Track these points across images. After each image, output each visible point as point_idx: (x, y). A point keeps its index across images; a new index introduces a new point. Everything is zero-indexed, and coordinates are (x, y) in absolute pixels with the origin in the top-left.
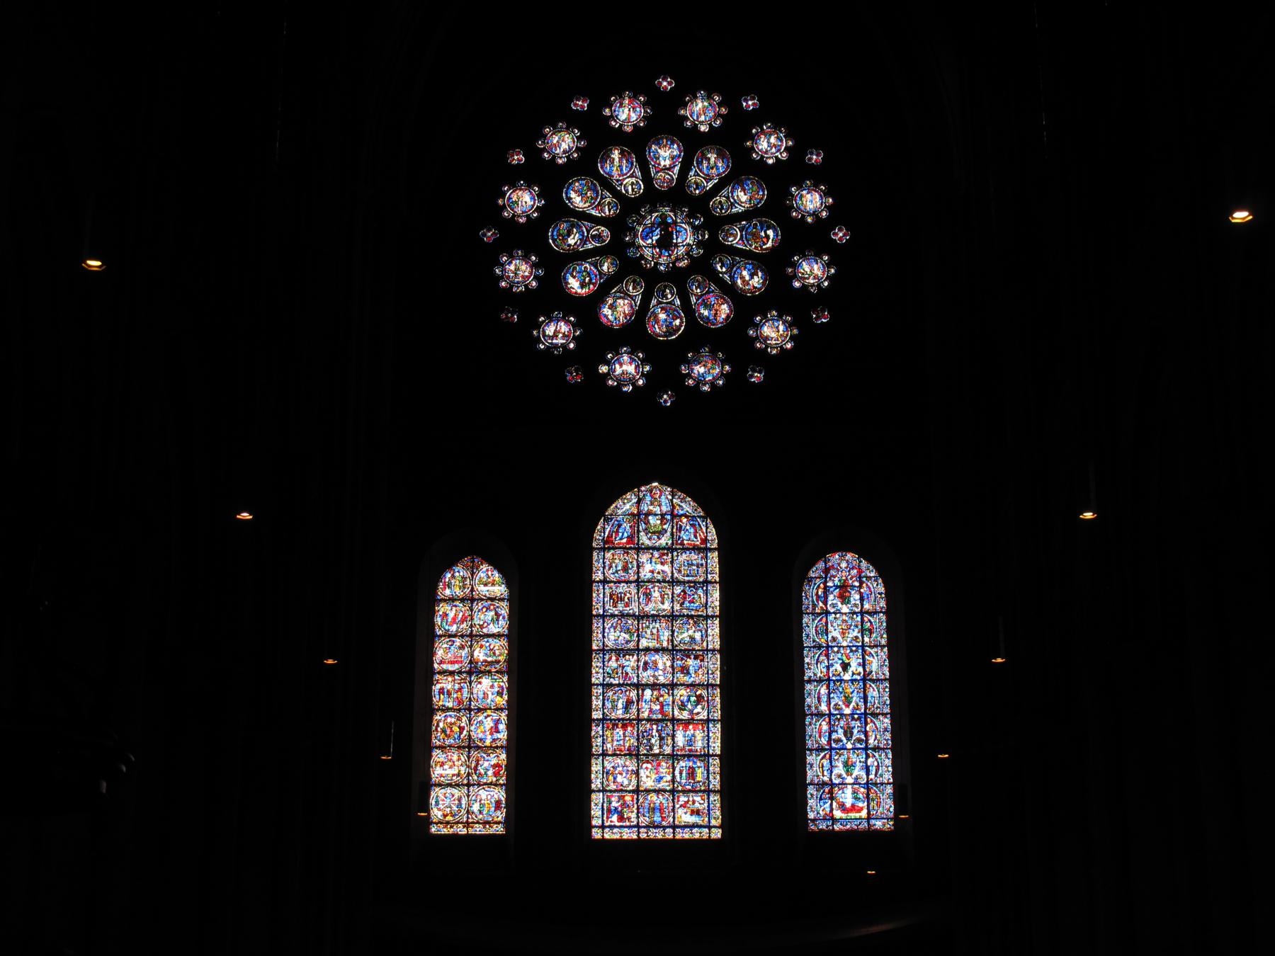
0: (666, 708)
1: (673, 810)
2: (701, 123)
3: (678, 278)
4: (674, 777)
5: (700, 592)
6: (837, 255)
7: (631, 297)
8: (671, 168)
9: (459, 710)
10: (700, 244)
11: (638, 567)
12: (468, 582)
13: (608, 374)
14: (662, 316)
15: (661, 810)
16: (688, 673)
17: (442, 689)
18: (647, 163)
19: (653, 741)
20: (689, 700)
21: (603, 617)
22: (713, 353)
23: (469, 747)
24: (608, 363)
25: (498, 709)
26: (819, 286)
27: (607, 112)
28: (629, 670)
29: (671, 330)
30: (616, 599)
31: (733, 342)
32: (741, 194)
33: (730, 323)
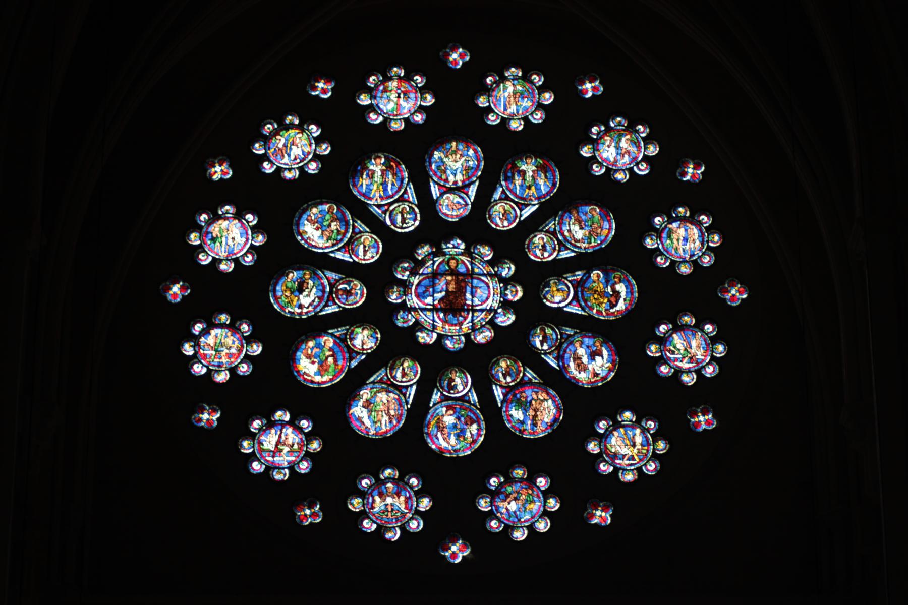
2: (512, 117)
3: (476, 360)
14: (449, 420)
31: (564, 459)
32: (575, 228)
33: (559, 430)
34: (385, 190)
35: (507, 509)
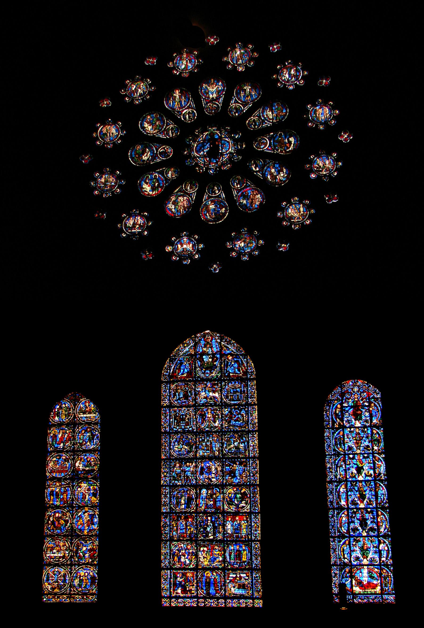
0: (218, 504)
1: (224, 585)
2: (239, 65)
4: (225, 558)
5: (243, 412)
6: (343, 152)
7: (189, 194)
8: (217, 99)
9: (65, 507)
10: (238, 152)
11: (196, 395)
12: (71, 411)
13: (172, 252)
14: (212, 207)
15: (215, 583)
16: (235, 476)
17: (52, 491)
18: (200, 97)
19: (208, 529)
20: (235, 497)
21: (169, 433)
22: (250, 233)
23: (72, 536)
24: (172, 244)
25: (93, 507)
26: (330, 175)
27: (171, 65)
28: (189, 474)
29: (219, 216)
30: (179, 419)
31: (265, 221)
34: (181, 104)
35: (239, 245)
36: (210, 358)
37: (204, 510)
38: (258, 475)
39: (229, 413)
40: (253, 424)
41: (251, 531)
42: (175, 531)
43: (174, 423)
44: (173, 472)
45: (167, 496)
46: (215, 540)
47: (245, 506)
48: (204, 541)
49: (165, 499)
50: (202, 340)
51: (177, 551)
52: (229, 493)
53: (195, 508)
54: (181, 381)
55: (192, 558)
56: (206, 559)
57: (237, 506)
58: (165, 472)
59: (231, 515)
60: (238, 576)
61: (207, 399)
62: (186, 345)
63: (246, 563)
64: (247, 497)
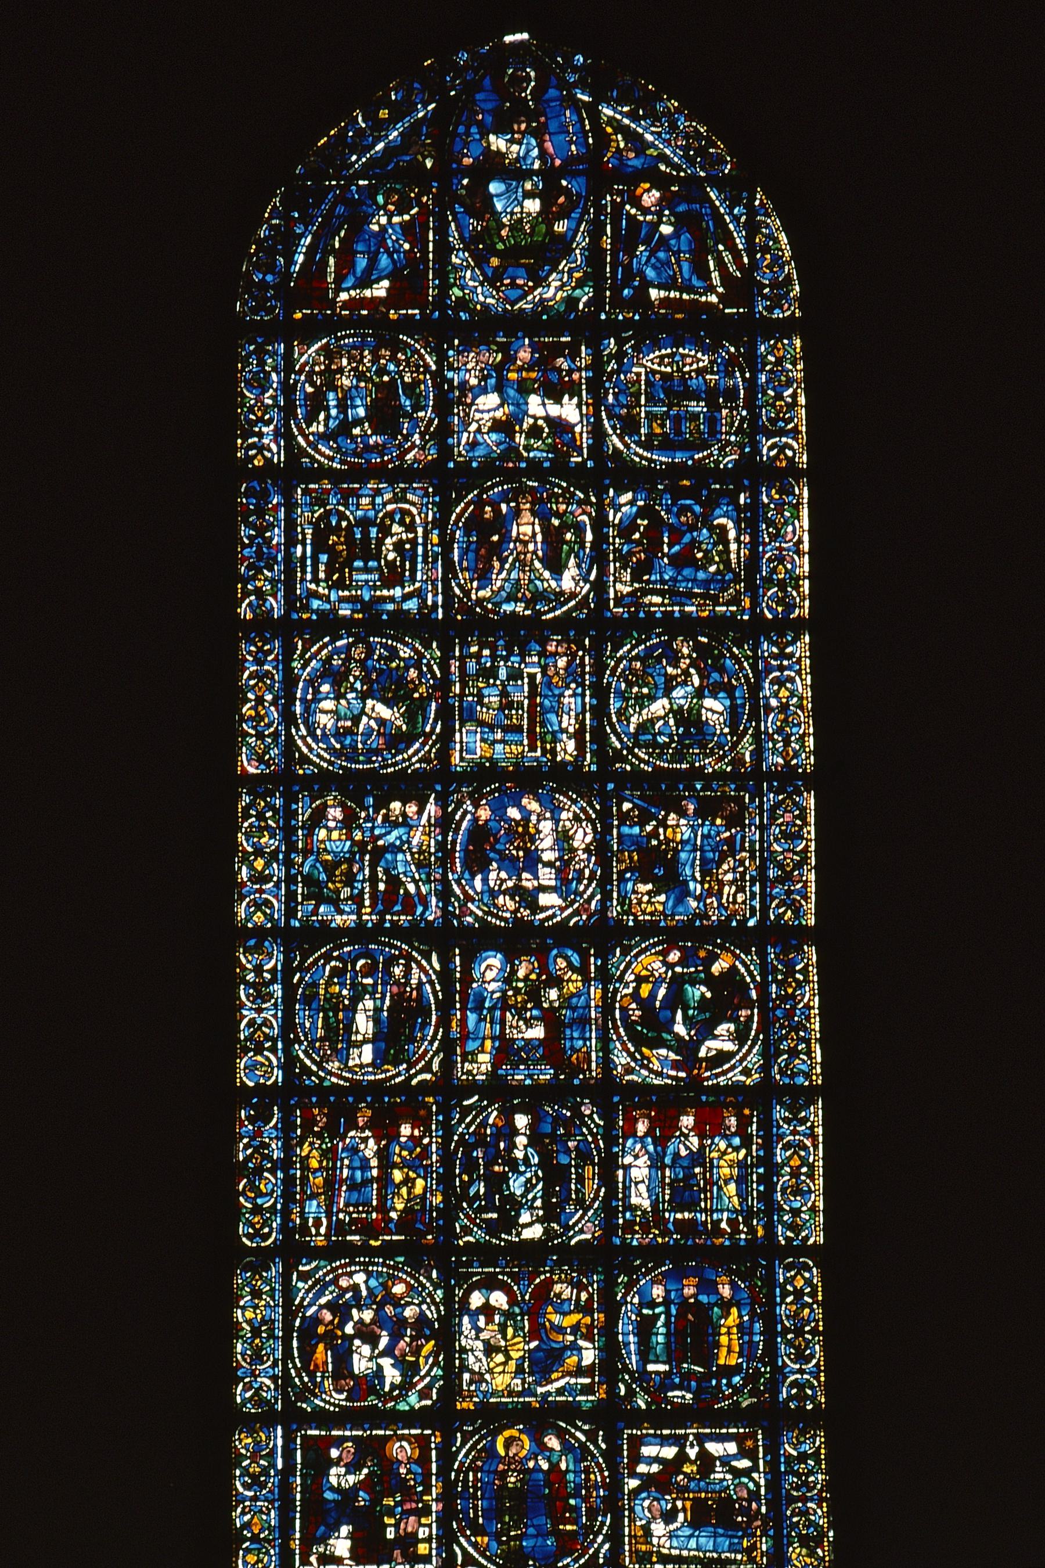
11: (444, 407)
19: (516, 1186)
20: (676, 999)
36: (528, 195)
37: (492, 1075)
38: (812, 877)
39: (641, 513)
40: (782, 585)
41: (767, 1197)
42: (314, 1196)
43: (315, 571)
44: (306, 852)
45: (271, 995)
46: (555, 1250)
47: (730, 1055)
48: (483, 1253)
49: (259, 1011)
50: (481, 89)
51: (328, 1316)
52: (640, 980)
53: (435, 1067)
54: (354, 323)
55: (417, 1352)
56: (500, 1358)
57: (687, 1050)
58: (259, 852)
59: (649, 1106)
60: (692, 1453)
61: (510, 434)
62: (384, 114)
63: (736, 1379)
64: (750, 1004)
